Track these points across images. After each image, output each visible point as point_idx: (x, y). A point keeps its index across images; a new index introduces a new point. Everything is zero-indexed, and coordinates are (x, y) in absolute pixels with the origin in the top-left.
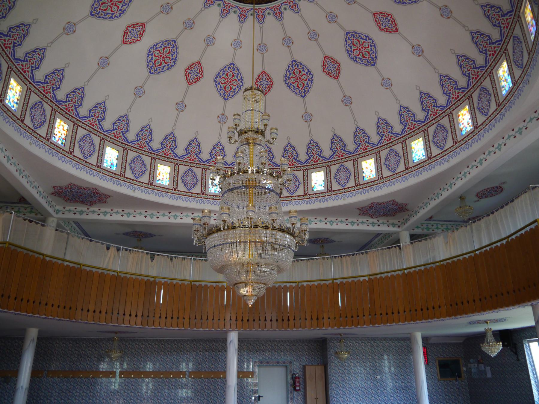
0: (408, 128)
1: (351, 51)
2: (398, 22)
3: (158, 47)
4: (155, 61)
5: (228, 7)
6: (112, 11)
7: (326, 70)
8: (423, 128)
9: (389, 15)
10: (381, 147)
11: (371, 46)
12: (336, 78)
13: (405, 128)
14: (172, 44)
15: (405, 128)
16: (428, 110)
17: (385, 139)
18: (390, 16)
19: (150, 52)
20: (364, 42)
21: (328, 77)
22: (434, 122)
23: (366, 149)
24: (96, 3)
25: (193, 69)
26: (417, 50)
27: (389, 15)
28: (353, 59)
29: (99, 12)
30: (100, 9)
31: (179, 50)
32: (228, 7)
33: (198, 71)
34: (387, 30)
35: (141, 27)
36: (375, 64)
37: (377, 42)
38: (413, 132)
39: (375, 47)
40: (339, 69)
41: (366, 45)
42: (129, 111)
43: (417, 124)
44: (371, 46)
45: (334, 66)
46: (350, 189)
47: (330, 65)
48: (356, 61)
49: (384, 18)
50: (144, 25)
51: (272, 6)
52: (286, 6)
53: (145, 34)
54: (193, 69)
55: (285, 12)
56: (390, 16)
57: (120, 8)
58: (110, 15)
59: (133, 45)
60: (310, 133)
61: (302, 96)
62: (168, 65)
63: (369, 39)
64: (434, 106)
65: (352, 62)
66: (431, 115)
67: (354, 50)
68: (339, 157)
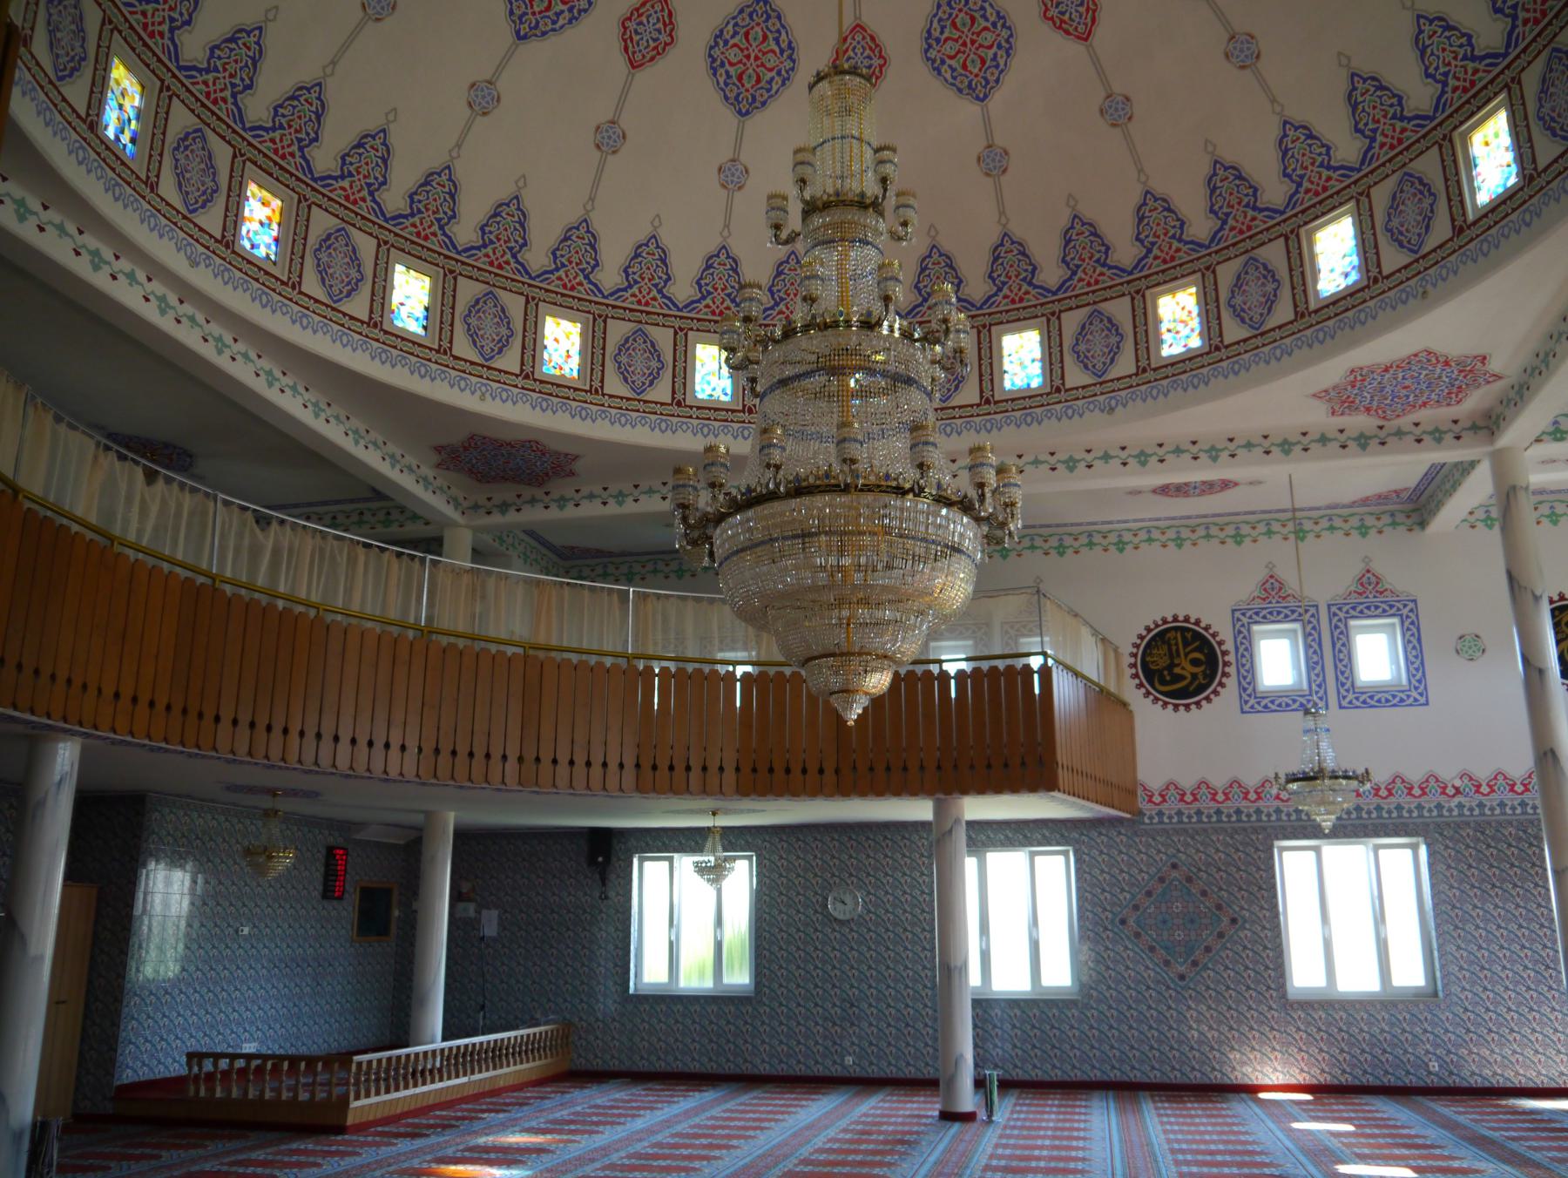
0: (707, 306)
1: (726, 42)
7: (631, 25)
10: (614, 307)
11: (779, 73)
13: (698, 301)
15: (698, 301)
17: (634, 295)
20: (773, 51)
23: (573, 288)
28: (714, 60)
36: (747, 113)
40: (659, 51)
41: (771, 61)
44: (779, 73)
46: (503, 377)
60: (459, 146)
61: (518, 33)
63: (790, 57)
65: (702, 65)
66: (781, 312)
67: (735, 45)
68: (491, 264)
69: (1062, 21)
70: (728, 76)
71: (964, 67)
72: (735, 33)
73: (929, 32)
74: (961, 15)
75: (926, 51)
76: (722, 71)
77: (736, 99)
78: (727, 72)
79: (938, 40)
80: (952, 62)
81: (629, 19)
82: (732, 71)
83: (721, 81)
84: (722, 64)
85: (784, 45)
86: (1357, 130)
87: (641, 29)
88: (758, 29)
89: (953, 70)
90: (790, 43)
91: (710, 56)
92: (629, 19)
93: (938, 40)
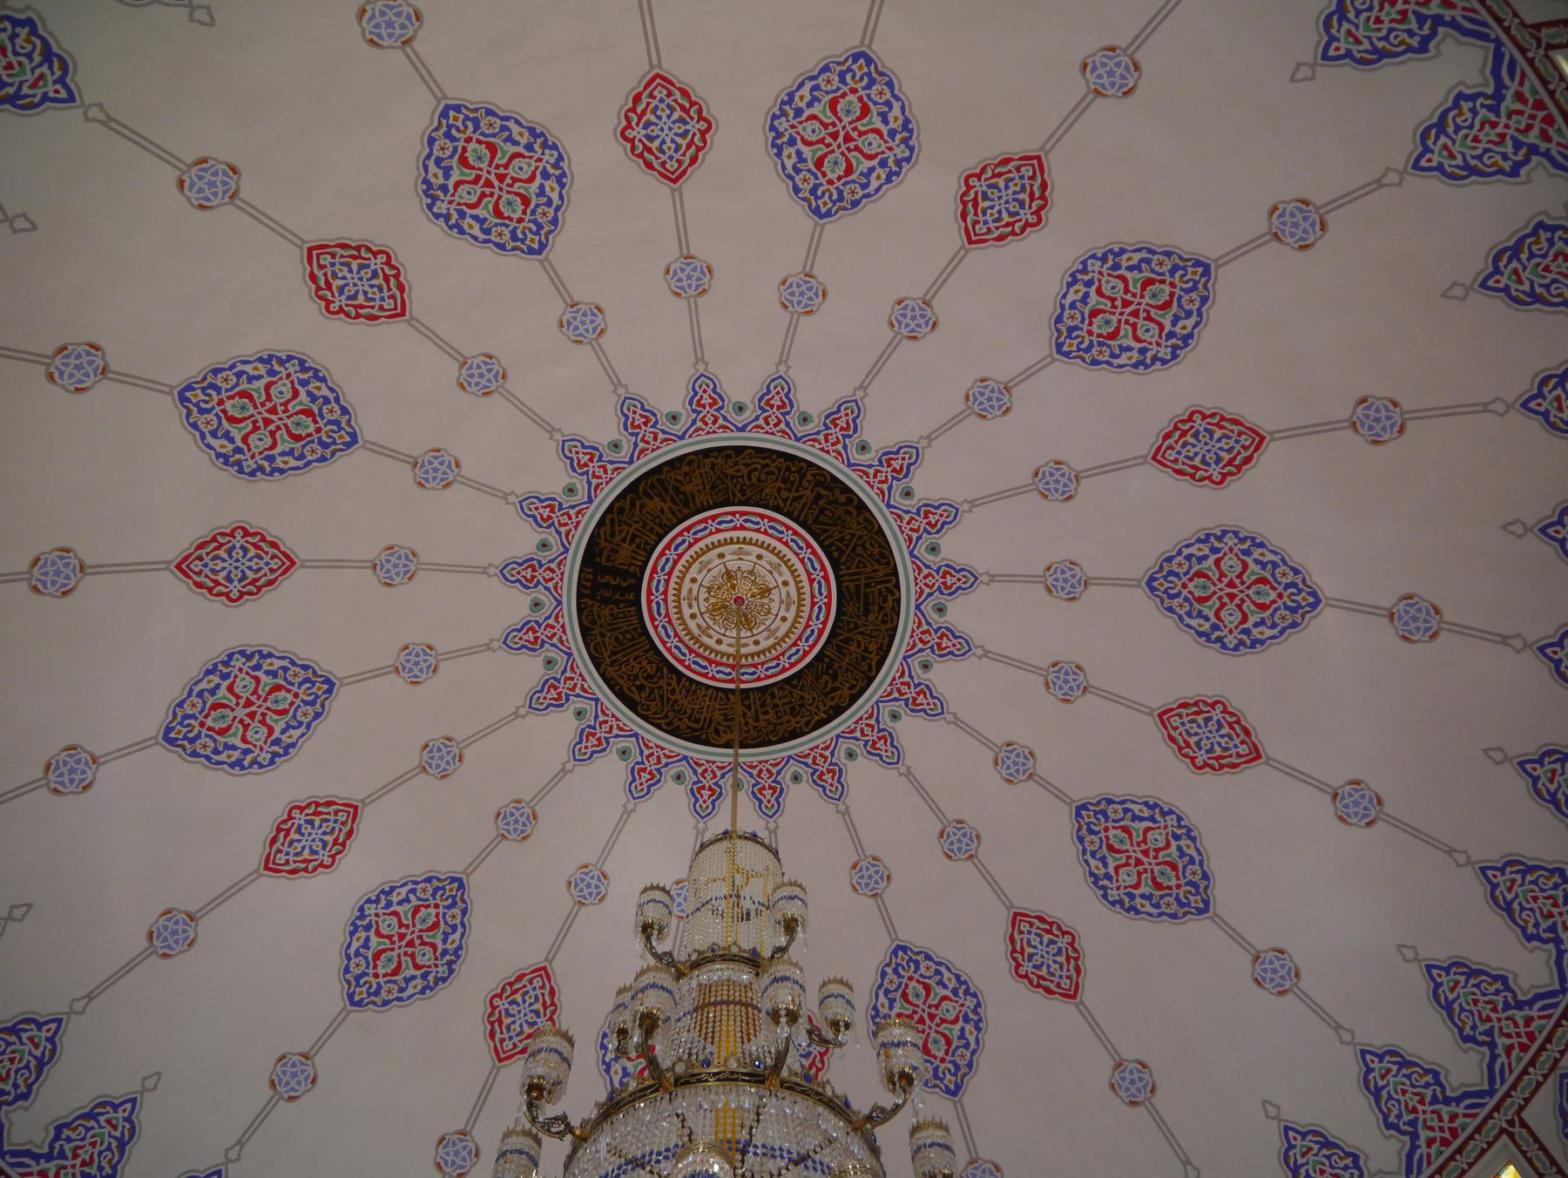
2: (1252, 718)
3: (395, 898)
4: (377, 956)
5: (653, 760)
6: (244, 740)
7: (1027, 967)
8: (1500, 1120)
9: (1213, 705)
11: (1177, 837)
12: (1071, 995)
13: (1414, 1147)
14: (451, 892)
16: (1489, 1033)
18: (1219, 708)
19: (362, 917)
20: (1147, 830)
21: (1039, 997)
22: (1535, 1075)
24: (194, 699)
25: (518, 997)
26: (1356, 804)
27: (1213, 705)
28: (1121, 902)
29: (198, 736)
30: (202, 724)
31: (474, 919)
32: (653, 760)
33: (538, 1006)
34: (1219, 764)
35: (342, 817)
37: (1194, 817)
38: (1460, 1150)
39: (1193, 839)
40: (1074, 957)
42: (233, 1154)
43: (1460, 1110)
44: (1177, 837)
45: (1053, 949)
47: (1039, 947)
48: (1132, 909)
49: (1200, 719)
50: (354, 810)
51: (805, 749)
52: (852, 745)
53: (355, 845)
54: (518, 997)
55: (850, 764)
56: (1219, 708)
57: (276, 734)
58: (236, 755)
59: (304, 883)
61: (948, 1091)
62: (425, 976)
63: (1164, 814)
64: (1507, 1006)
66: (1509, 1049)
67: (1117, 869)
69: (1230, 463)
70: (1149, 897)
71: (1263, 607)
72: (1103, 860)
73: (1201, 634)
74: (1191, 586)
75: (1224, 646)
76: (1138, 901)
77: (1181, 905)
78: (1143, 896)
79: (1215, 627)
80: (1252, 620)
81: (1018, 965)
82: (1143, 889)
83: (1149, 908)
84: (1132, 897)
85: (1147, 813)
86: (1423, 47)
87: (1037, 960)
88: (1111, 833)
89: (1262, 623)
90: (1146, 804)
91: (1113, 903)
92: (1018, 965)
93: (1215, 627)
